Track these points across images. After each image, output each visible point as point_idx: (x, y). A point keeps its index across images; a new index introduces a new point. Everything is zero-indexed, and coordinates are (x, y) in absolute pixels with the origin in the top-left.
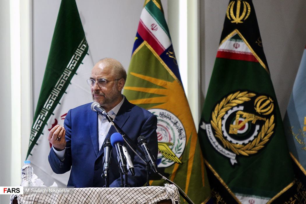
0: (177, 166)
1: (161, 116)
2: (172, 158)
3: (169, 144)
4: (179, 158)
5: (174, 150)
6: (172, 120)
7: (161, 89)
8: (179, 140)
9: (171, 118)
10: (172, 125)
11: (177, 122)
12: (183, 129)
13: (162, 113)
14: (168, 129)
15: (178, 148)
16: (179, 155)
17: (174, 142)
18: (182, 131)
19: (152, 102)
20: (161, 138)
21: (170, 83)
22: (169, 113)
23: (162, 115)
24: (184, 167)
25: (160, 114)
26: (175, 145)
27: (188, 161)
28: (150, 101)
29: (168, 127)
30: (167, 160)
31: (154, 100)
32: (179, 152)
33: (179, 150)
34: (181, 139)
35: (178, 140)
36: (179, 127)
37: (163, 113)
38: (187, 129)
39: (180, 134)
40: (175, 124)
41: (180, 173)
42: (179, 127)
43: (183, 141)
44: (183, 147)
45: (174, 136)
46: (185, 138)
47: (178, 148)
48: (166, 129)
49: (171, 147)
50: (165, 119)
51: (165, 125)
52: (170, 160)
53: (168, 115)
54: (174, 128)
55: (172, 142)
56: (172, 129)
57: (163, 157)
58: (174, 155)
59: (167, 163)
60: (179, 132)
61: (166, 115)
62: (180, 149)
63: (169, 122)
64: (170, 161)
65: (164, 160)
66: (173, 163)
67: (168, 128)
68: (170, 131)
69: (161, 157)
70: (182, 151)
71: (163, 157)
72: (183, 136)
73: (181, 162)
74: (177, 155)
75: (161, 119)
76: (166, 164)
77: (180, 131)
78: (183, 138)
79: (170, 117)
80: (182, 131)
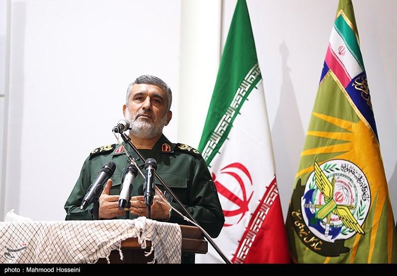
0: (358, 236)
1: (342, 168)
2: (353, 226)
3: (350, 208)
4: (361, 227)
5: (355, 215)
6: (356, 174)
8: (362, 200)
9: (355, 172)
10: (355, 181)
11: (362, 177)
12: (368, 187)
13: (344, 166)
14: (350, 186)
15: (360, 212)
16: (361, 222)
17: (356, 205)
18: (366, 189)
19: (334, 151)
20: (342, 200)
21: (355, 124)
22: (353, 165)
23: (344, 167)
24: (367, 235)
25: (342, 167)
26: (357, 209)
27: (371, 231)
28: (332, 149)
29: (351, 184)
30: (348, 229)
31: (336, 148)
32: (360, 218)
33: (361, 216)
34: (365, 200)
35: (361, 201)
36: (363, 184)
37: (345, 164)
38: (371, 187)
39: (364, 194)
40: (359, 180)
41: (362, 248)
42: (363, 184)
43: (367, 204)
44: (366, 211)
45: (357, 196)
46: (369, 199)
47: (360, 212)
48: (347, 187)
49: (352, 211)
50: (347, 173)
51: (347, 181)
52: (351, 228)
53: (351, 168)
54: (358, 185)
55: (354, 204)
56: (355, 187)
57: (343, 225)
58: (356, 223)
59: (348, 233)
60: (362, 190)
61: (349, 168)
62: (363, 214)
63: (352, 177)
64: (351, 230)
65: (345, 230)
66: (354, 232)
67: (351, 185)
68: (353, 189)
69: (341, 226)
70: (364, 216)
71: (343, 225)
72: (367, 196)
73: (363, 233)
74: (358, 221)
75: (343, 173)
76: (346, 234)
77: (364, 190)
78: (367, 199)
79: (353, 170)
80: (366, 189)
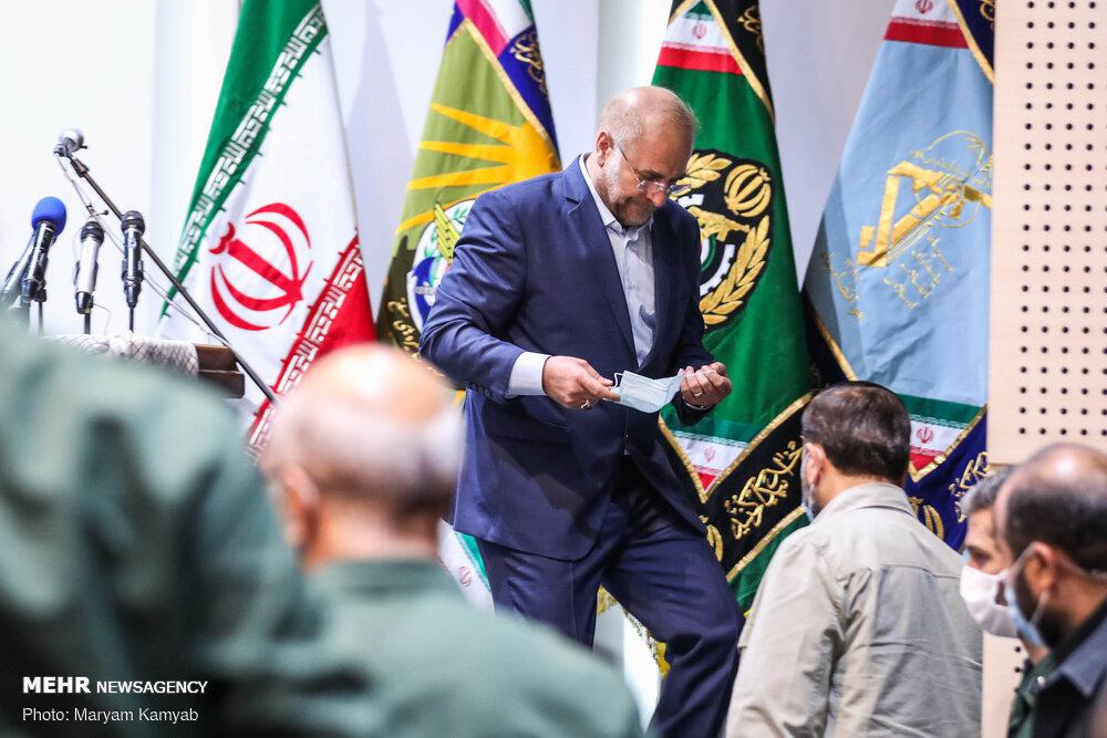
7: (496, 148)
19: (475, 182)
28: (468, 178)
